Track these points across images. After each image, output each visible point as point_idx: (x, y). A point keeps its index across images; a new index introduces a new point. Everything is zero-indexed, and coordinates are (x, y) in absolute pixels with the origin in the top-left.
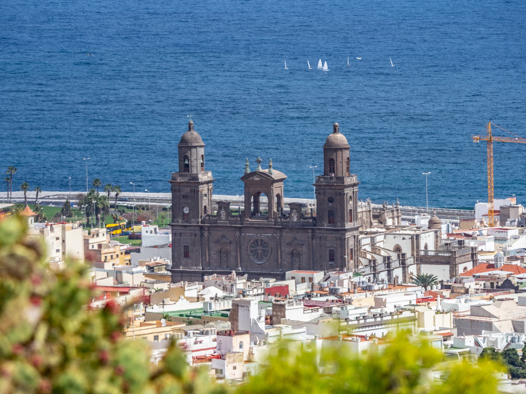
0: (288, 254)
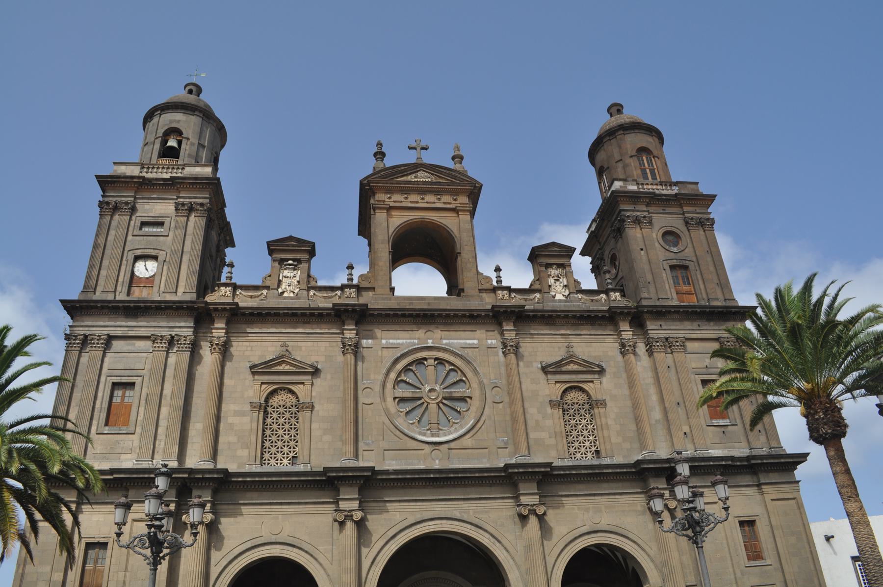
0: (552, 403)
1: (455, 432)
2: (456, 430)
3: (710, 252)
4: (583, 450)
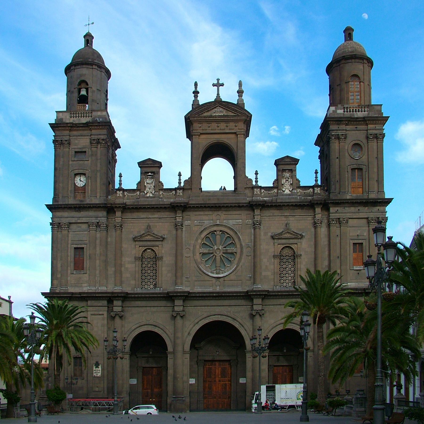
0: (274, 257)
1: (227, 272)
2: (228, 271)
3: (377, 158)
4: (287, 281)
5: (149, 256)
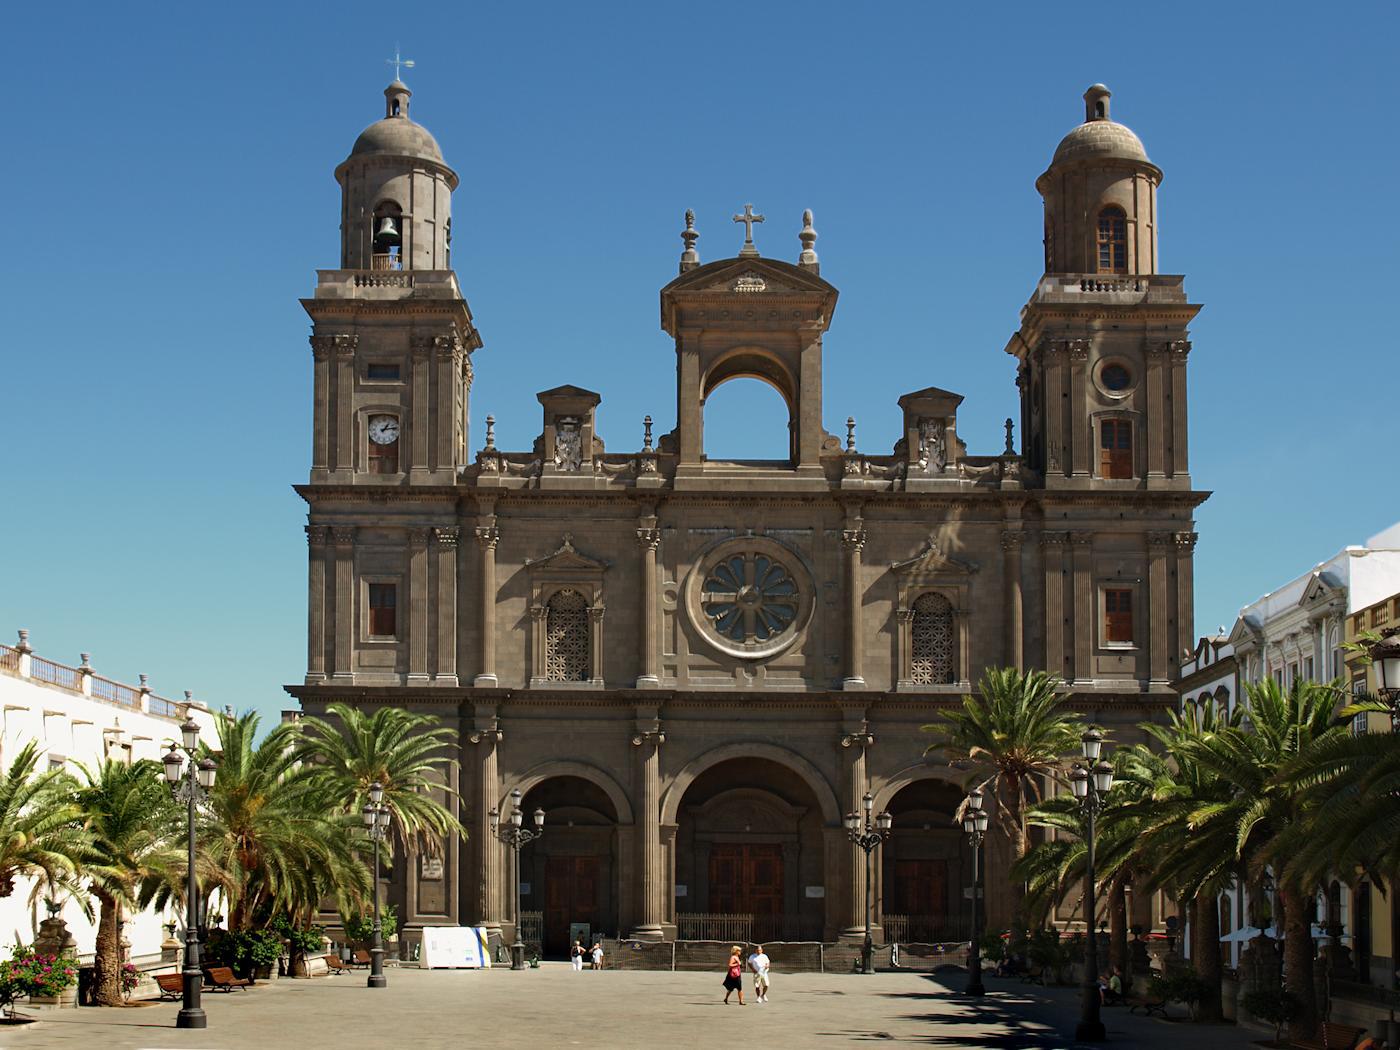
5: (567, 607)
